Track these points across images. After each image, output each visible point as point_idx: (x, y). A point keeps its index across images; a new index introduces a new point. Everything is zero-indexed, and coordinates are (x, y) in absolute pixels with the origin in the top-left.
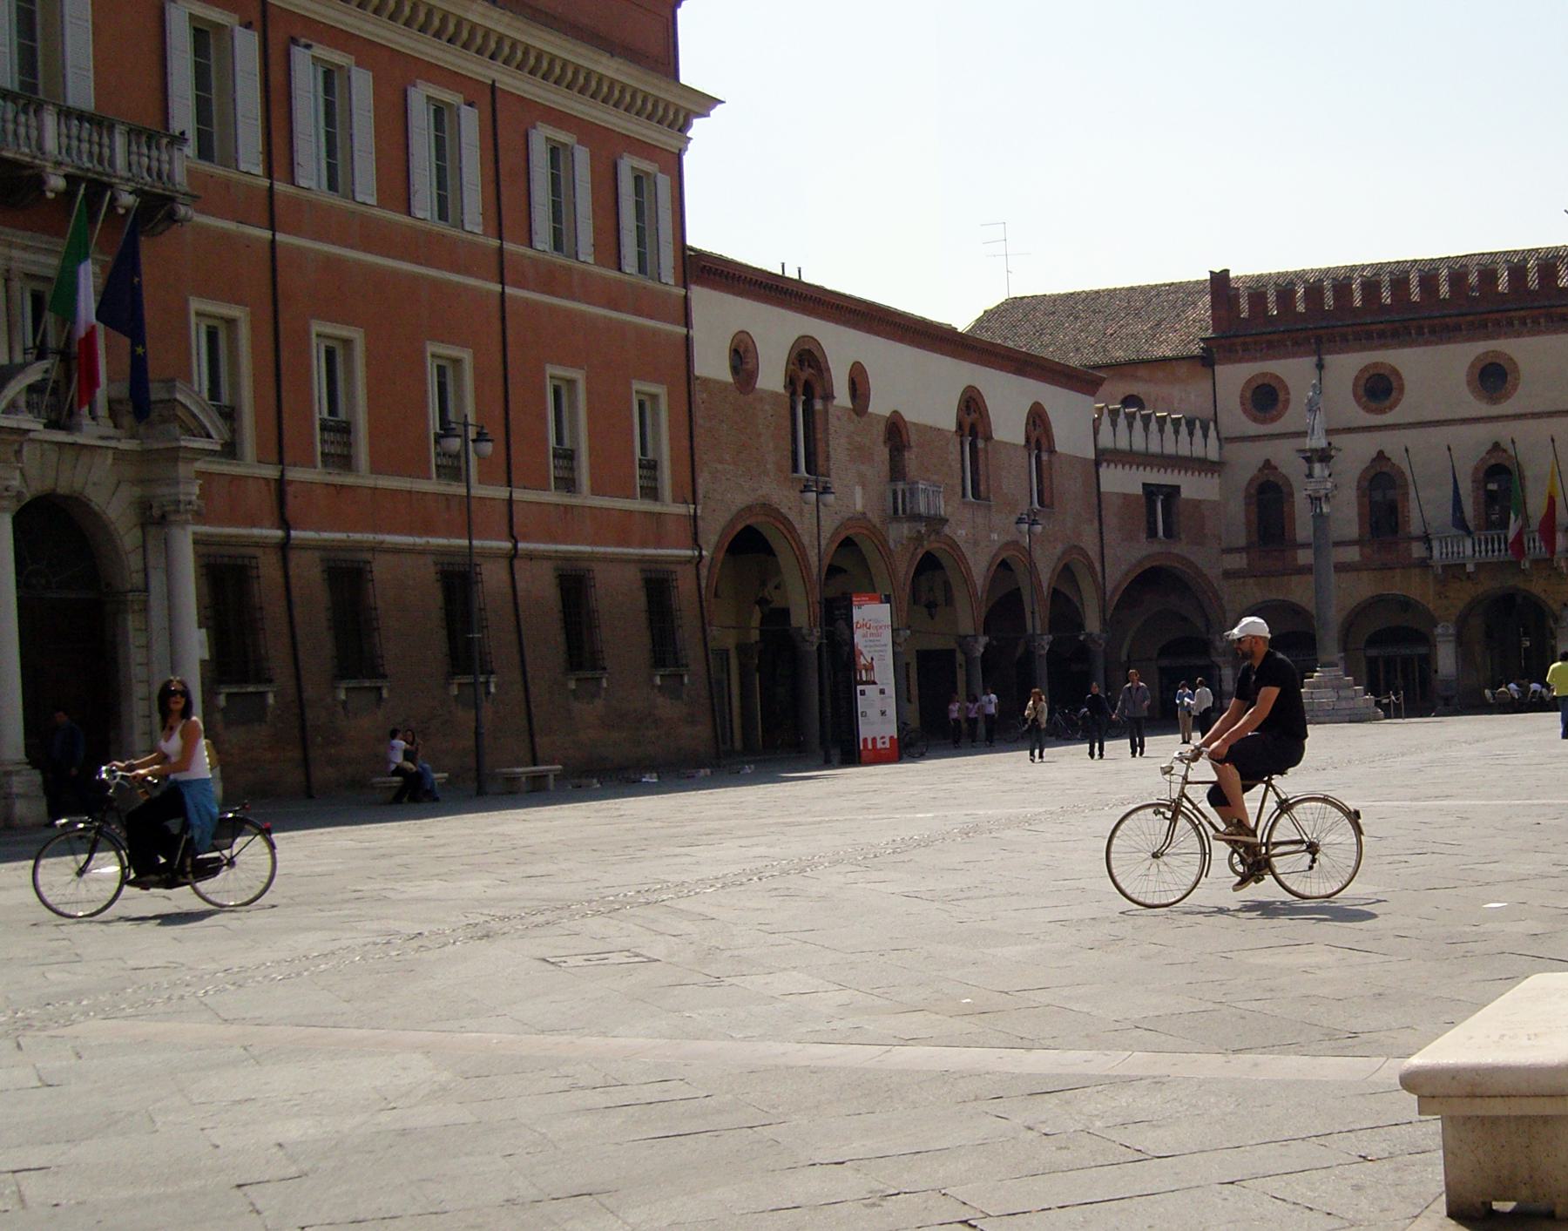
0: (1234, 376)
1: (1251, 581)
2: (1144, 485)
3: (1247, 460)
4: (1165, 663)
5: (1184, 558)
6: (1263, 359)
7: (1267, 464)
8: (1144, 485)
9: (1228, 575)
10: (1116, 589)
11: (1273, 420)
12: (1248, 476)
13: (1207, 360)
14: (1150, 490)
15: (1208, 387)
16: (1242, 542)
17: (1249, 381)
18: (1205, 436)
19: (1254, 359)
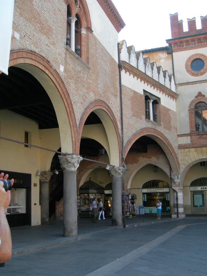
0: (182, 57)
1: (193, 150)
2: (144, 91)
3: (189, 94)
4: (145, 191)
5: (162, 134)
6: (195, 48)
7: (200, 94)
8: (144, 91)
9: (181, 147)
10: (129, 141)
11: (202, 74)
12: (191, 100)
13: (168, 50)
14: (147, 97)
15: (171, 61)
16: (188, 132)
17: (189, 58)
18: (170, 80)
19: (192, 48)
